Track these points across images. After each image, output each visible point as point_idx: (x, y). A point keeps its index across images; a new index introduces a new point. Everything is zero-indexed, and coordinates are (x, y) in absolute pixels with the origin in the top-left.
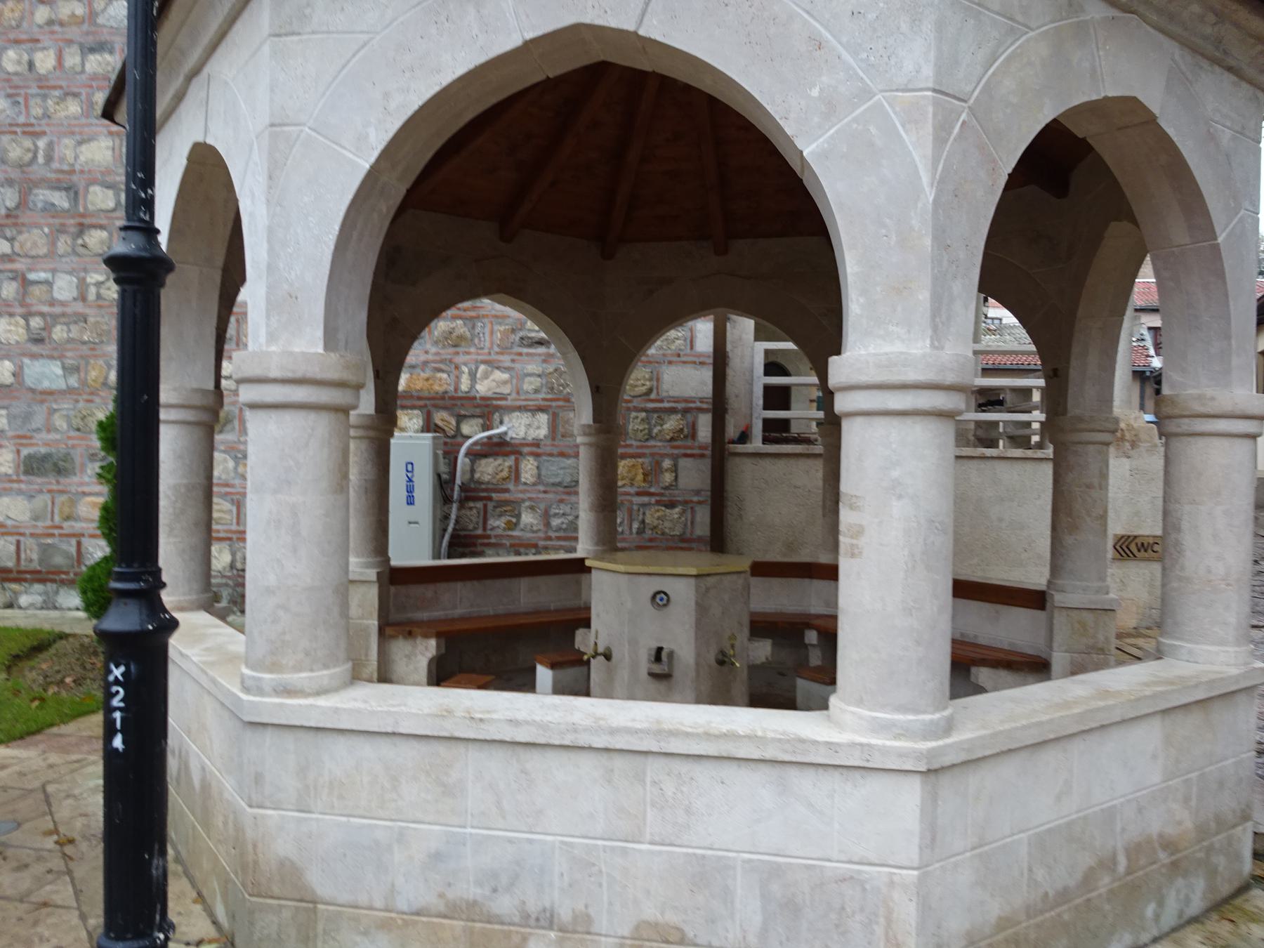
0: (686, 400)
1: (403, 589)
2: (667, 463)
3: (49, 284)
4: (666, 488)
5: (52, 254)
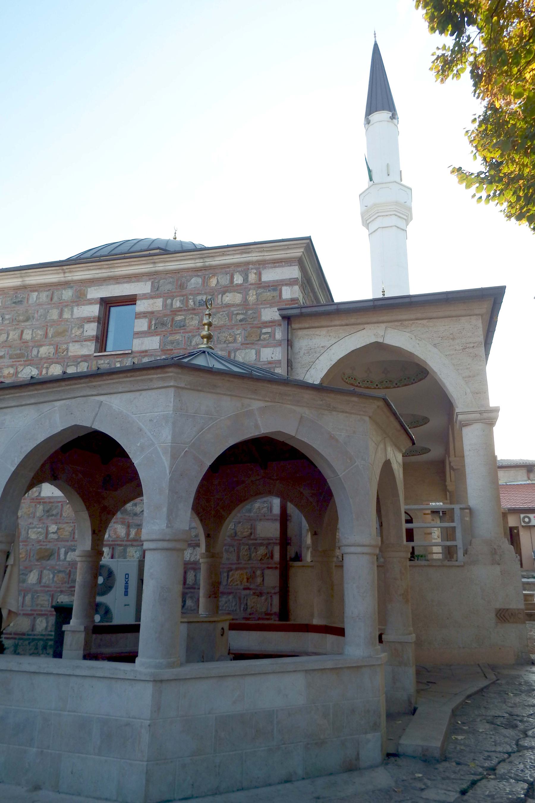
0: (268, 539)
1: (99, 636)
2: (258, 573)
4: (258, 586)
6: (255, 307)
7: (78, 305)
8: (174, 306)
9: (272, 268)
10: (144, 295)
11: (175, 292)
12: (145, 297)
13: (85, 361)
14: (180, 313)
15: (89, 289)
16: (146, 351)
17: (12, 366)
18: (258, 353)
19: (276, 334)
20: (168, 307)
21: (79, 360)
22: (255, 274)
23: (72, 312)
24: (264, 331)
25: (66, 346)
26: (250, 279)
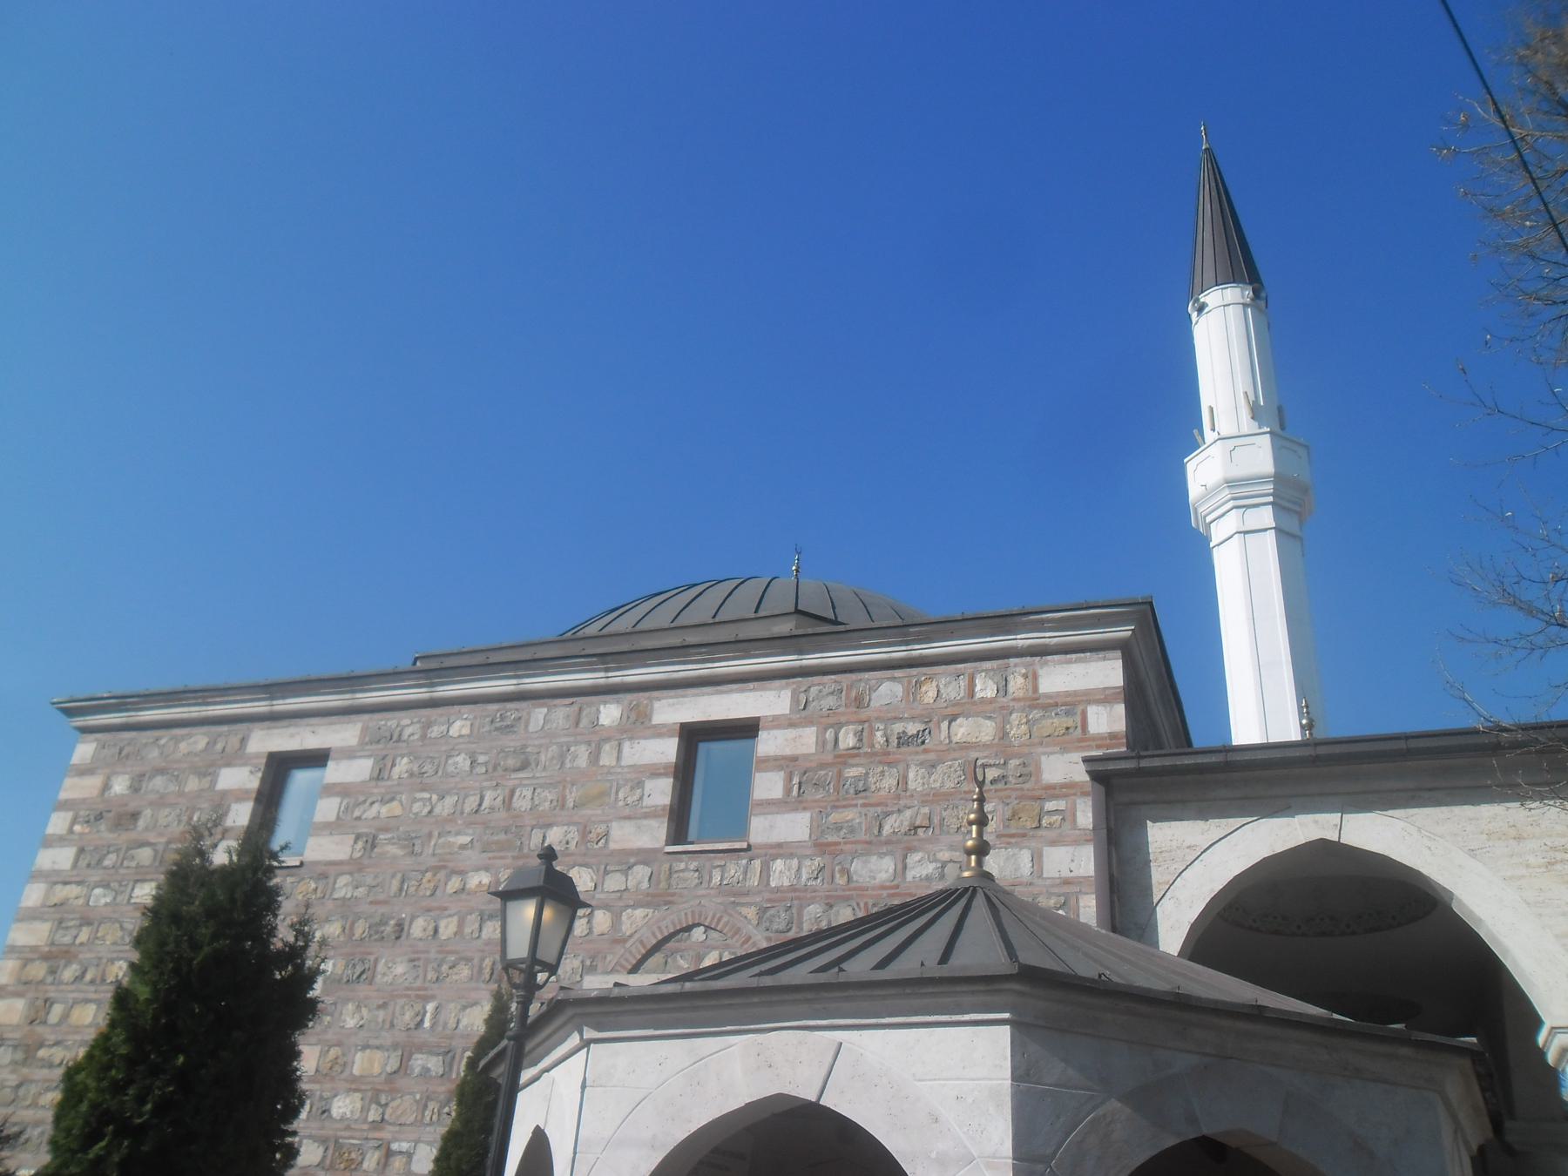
3: (409, 1155)
5: (419, 1122)
6: (1026, 750)
7: (631, 739)
8: (842, 745)
9: (1061, 663)
10: (775, 718)
11: (843, 714)
12: (778, 722)
13: (645, 863)
14: (856, 761)
15: (657, 705)
16: (780, 845)
17: (487, 869)
18: (1037, 858)
19: (1079, 814)
20: (830, 746)
21: (632, 860)
22: (1025, 676)
23: (620, 751)
24: (1050, 805)
25: (604, 827)
26: (1011, 688)
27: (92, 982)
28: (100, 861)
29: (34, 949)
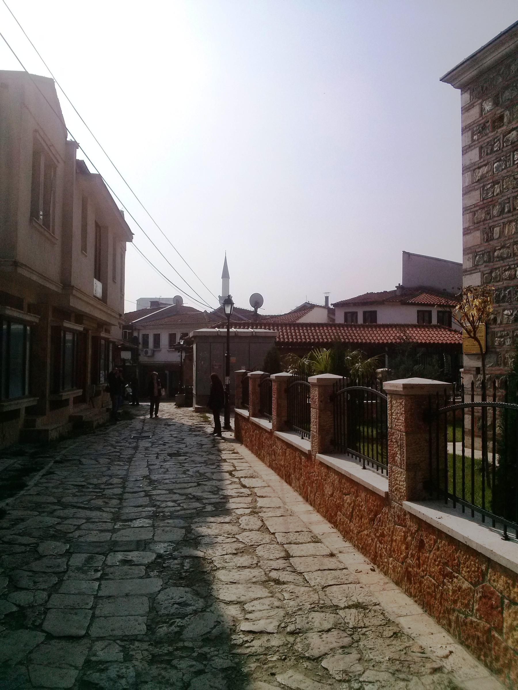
27: (509, 211)
28: (492, 149)
29: (475, 205)
